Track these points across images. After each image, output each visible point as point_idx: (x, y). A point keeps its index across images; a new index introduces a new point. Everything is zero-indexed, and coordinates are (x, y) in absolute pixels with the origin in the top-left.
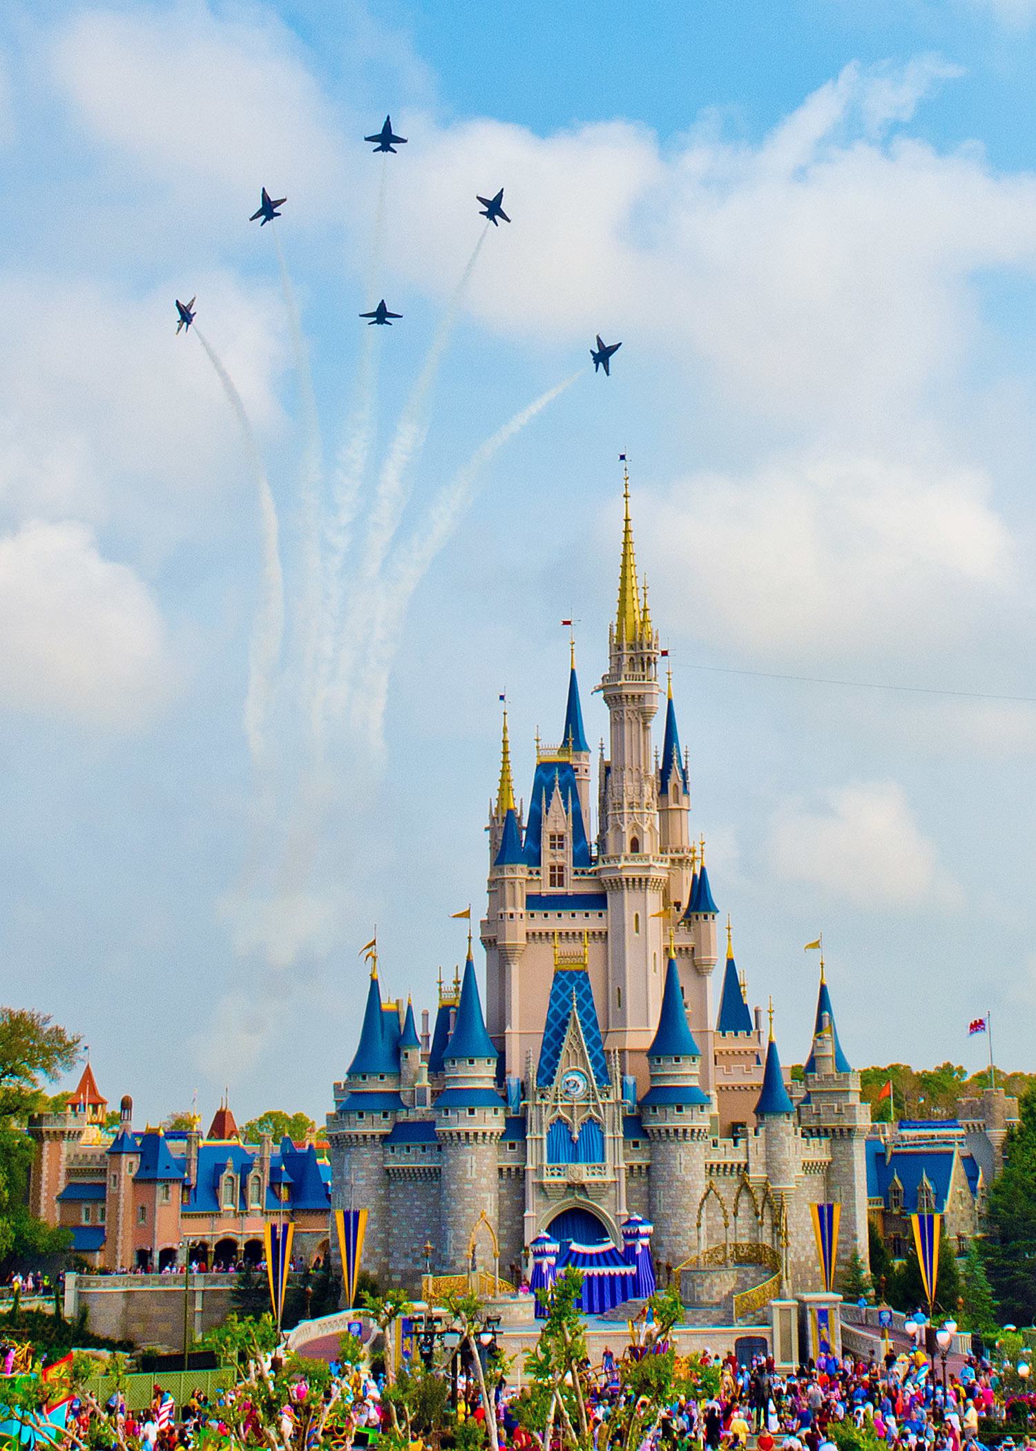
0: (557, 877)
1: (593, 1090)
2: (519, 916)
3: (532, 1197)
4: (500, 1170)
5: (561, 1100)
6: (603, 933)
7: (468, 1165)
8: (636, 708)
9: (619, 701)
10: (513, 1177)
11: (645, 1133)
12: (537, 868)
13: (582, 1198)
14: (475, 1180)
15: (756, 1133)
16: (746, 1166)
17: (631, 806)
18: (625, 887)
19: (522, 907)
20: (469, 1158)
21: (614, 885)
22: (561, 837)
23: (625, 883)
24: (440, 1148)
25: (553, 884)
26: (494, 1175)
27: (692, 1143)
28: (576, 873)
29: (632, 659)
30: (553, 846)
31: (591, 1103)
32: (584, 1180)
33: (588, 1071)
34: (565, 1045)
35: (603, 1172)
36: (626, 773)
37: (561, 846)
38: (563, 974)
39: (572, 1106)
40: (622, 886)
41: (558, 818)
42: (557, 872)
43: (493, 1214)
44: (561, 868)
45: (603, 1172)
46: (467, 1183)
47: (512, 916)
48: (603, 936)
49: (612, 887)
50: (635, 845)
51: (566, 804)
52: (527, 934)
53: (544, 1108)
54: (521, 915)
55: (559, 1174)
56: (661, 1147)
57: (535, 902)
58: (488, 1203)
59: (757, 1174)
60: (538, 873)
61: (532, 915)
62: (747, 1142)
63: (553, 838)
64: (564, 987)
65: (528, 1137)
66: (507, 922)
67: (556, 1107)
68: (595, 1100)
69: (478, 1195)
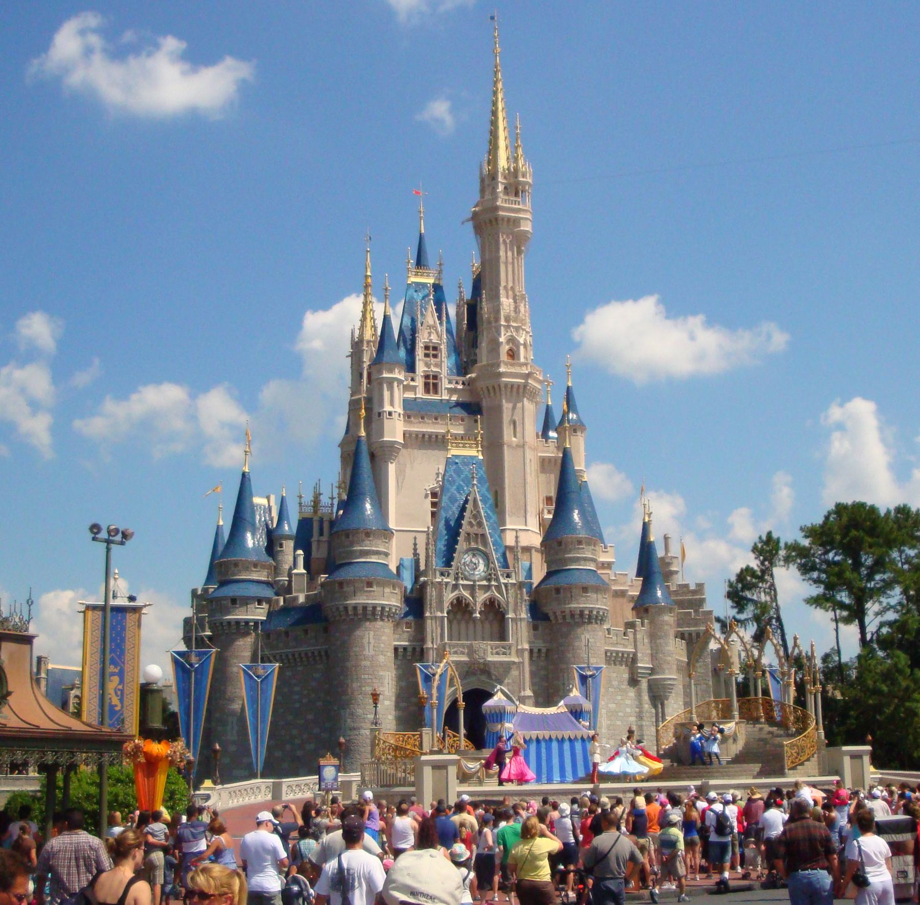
0: (431, 383)
2: (397, 415)
4: (396, 649)
5: (462, 579)
7: (365, 641)
9: (494, 223)
10: (410, 658)
11: (546, 618)
12: (411, 374)
14: (373, 656)
15: (643, 625)
16: (635, 654)
17: (507, 319)
18: (503, 392)
19: (400, 407)
20: (367, 633)
21: (491, 391)
24: (326, 630)
25: (427, 391)
26: (391, 654)
27: (596, 626)
28: (450, 382)
29: (505, 188)
30: (427, 355)
31: (493, 583)
32: (489, 659)
35: (508, 652)
37: (435, 356)
38: (456, 458)
42: (431, 381)
43: (391, 694)
44: (435, 377)
45: (508, 652)
47: (390, 414)
50: (513, 354)
51: (440, 318)
52: (404, 434)
53: (444, 586)
54: (399, 414)
58: (386, 681)
59: (644, 663)
60: (413, 380)
61: (409, 417)
62: (635, 634)
63: (427, 348)
65: (427, 614)
66: (386, 421)
67: (455, 587)
68: (497, 580)
69: (376, 673)
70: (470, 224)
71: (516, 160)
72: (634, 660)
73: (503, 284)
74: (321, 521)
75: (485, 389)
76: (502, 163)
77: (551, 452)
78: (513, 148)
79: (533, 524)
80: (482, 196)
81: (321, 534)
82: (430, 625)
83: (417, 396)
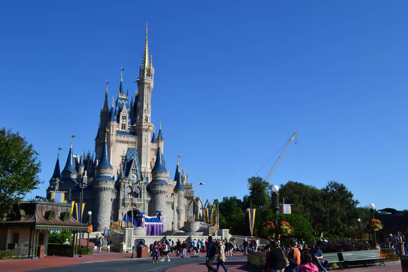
0: (124, 126)
3: (121, 207)
13: (134, 207)
25: (122, 129)
30: (123, 119)
34: (132, 168)
36: (144, 102)
57: (118, 132)
59: (176, 205)
63: (123, 116)
64: (131, 152)
70: (137, 83)
71: (150, 66)
72: (173, 204)
73: (145, 100)
74: (90, 162)
76: (147, 65)
77: (155, 146)
78: (150, 62)
79: (149, 166)
80: (140, 76)
81: (90, 165)
82: (122, 193)
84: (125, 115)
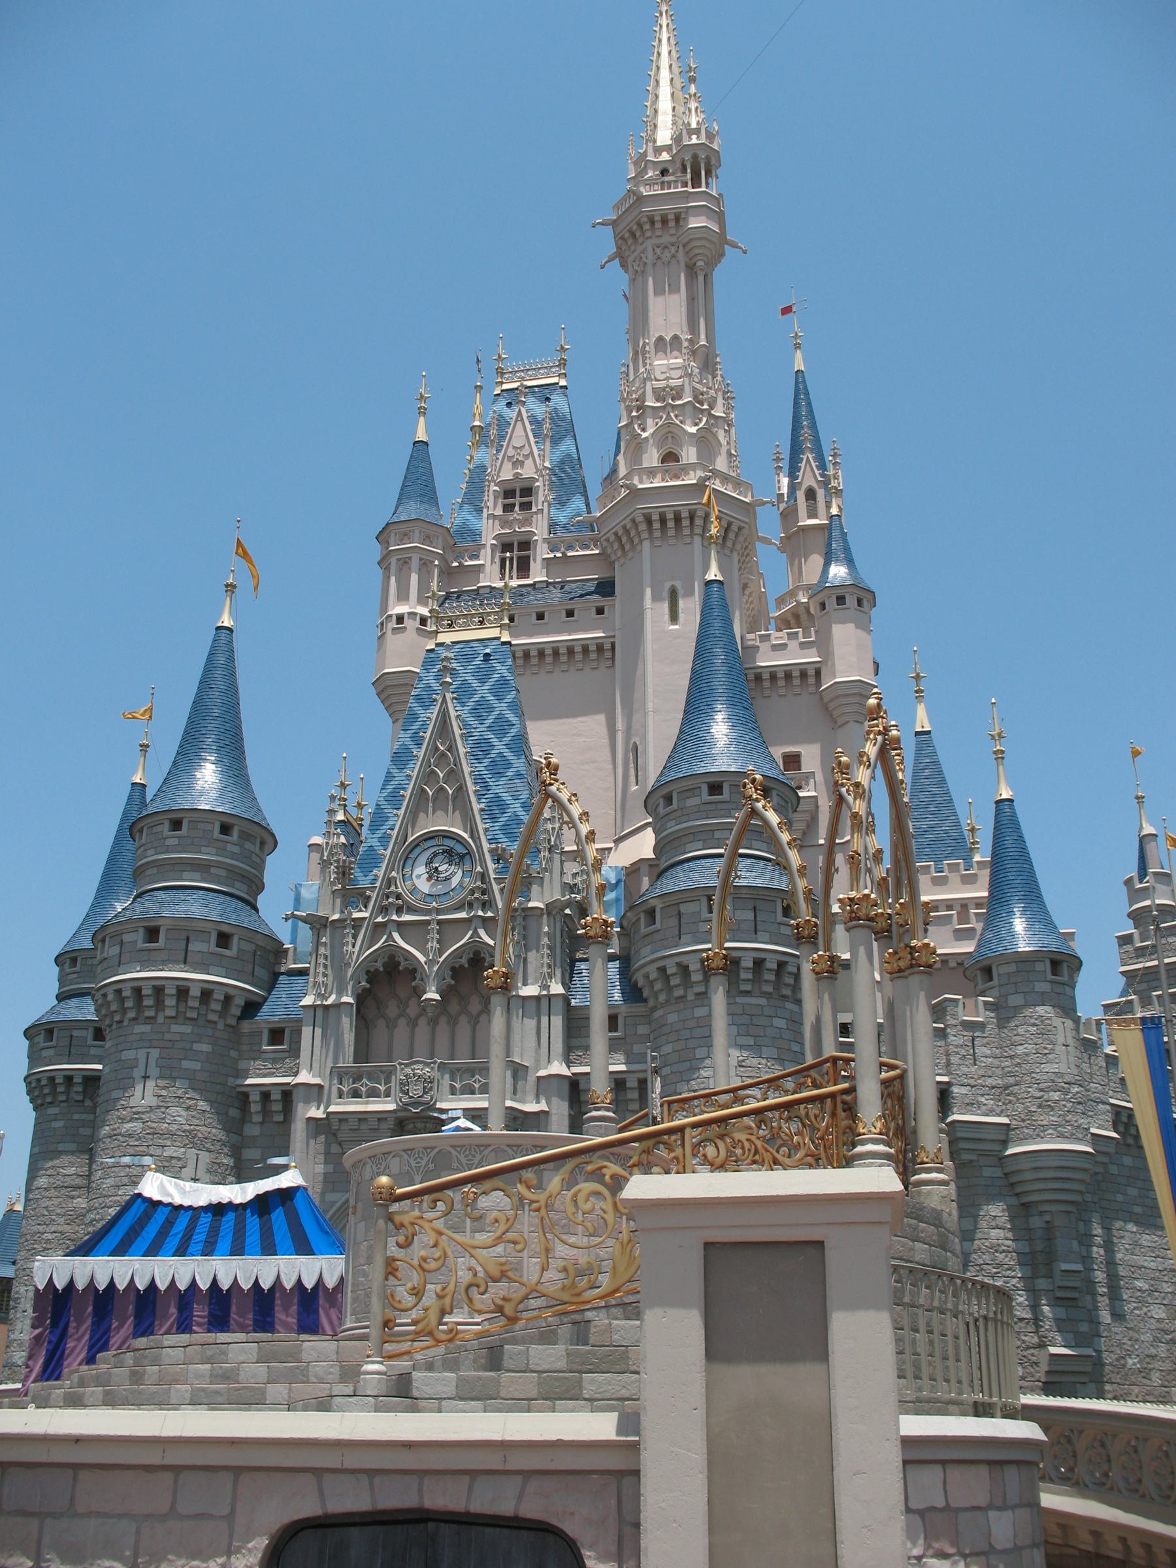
1: (483, 877)
6: (607, 646)
8: (673, 239)
17: (659, 395)
20: (142, 1054)
21: (624, 539)
22: (528, 491)
23: (643, 527)
30: (508, 508)
33: (473, 833)
39: (428, 922)
40: (639, 534)
41: (521, 458)
46: (131, 1120)
47: (400, 619)
48: (603, 651)
49: (622, 547)
55: (373, 1093)
56: (672, 1018)
63: (508, 493)
75: (612, 538)
83: (480, 585)
84: (528, 471)
